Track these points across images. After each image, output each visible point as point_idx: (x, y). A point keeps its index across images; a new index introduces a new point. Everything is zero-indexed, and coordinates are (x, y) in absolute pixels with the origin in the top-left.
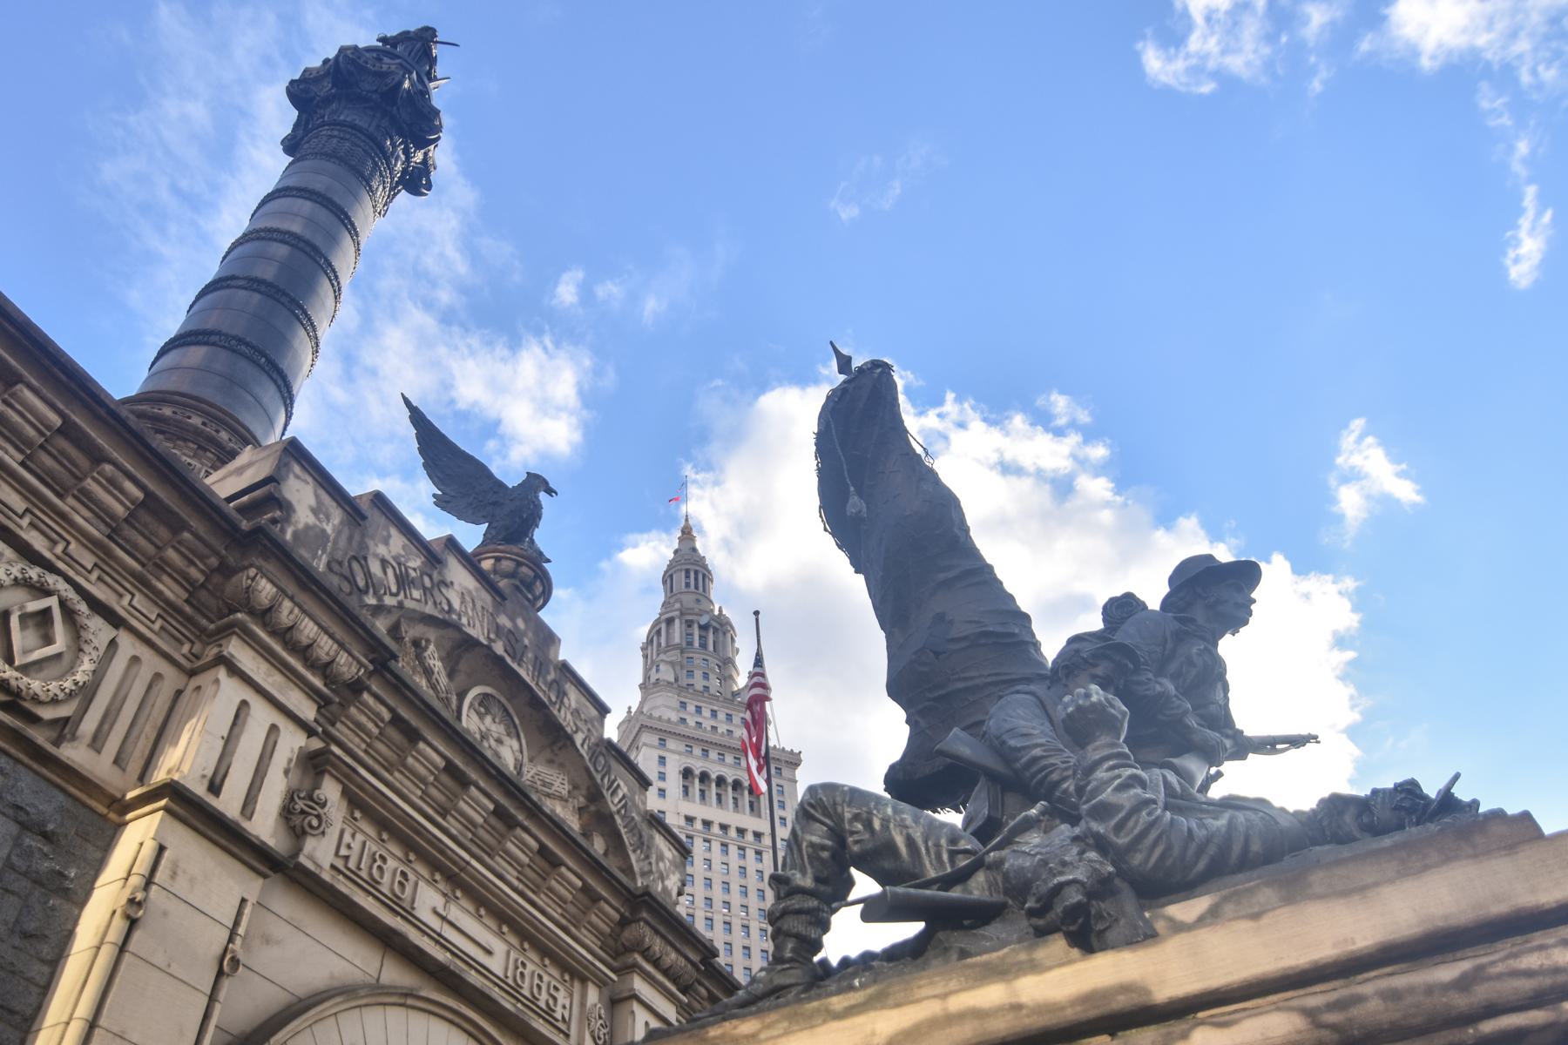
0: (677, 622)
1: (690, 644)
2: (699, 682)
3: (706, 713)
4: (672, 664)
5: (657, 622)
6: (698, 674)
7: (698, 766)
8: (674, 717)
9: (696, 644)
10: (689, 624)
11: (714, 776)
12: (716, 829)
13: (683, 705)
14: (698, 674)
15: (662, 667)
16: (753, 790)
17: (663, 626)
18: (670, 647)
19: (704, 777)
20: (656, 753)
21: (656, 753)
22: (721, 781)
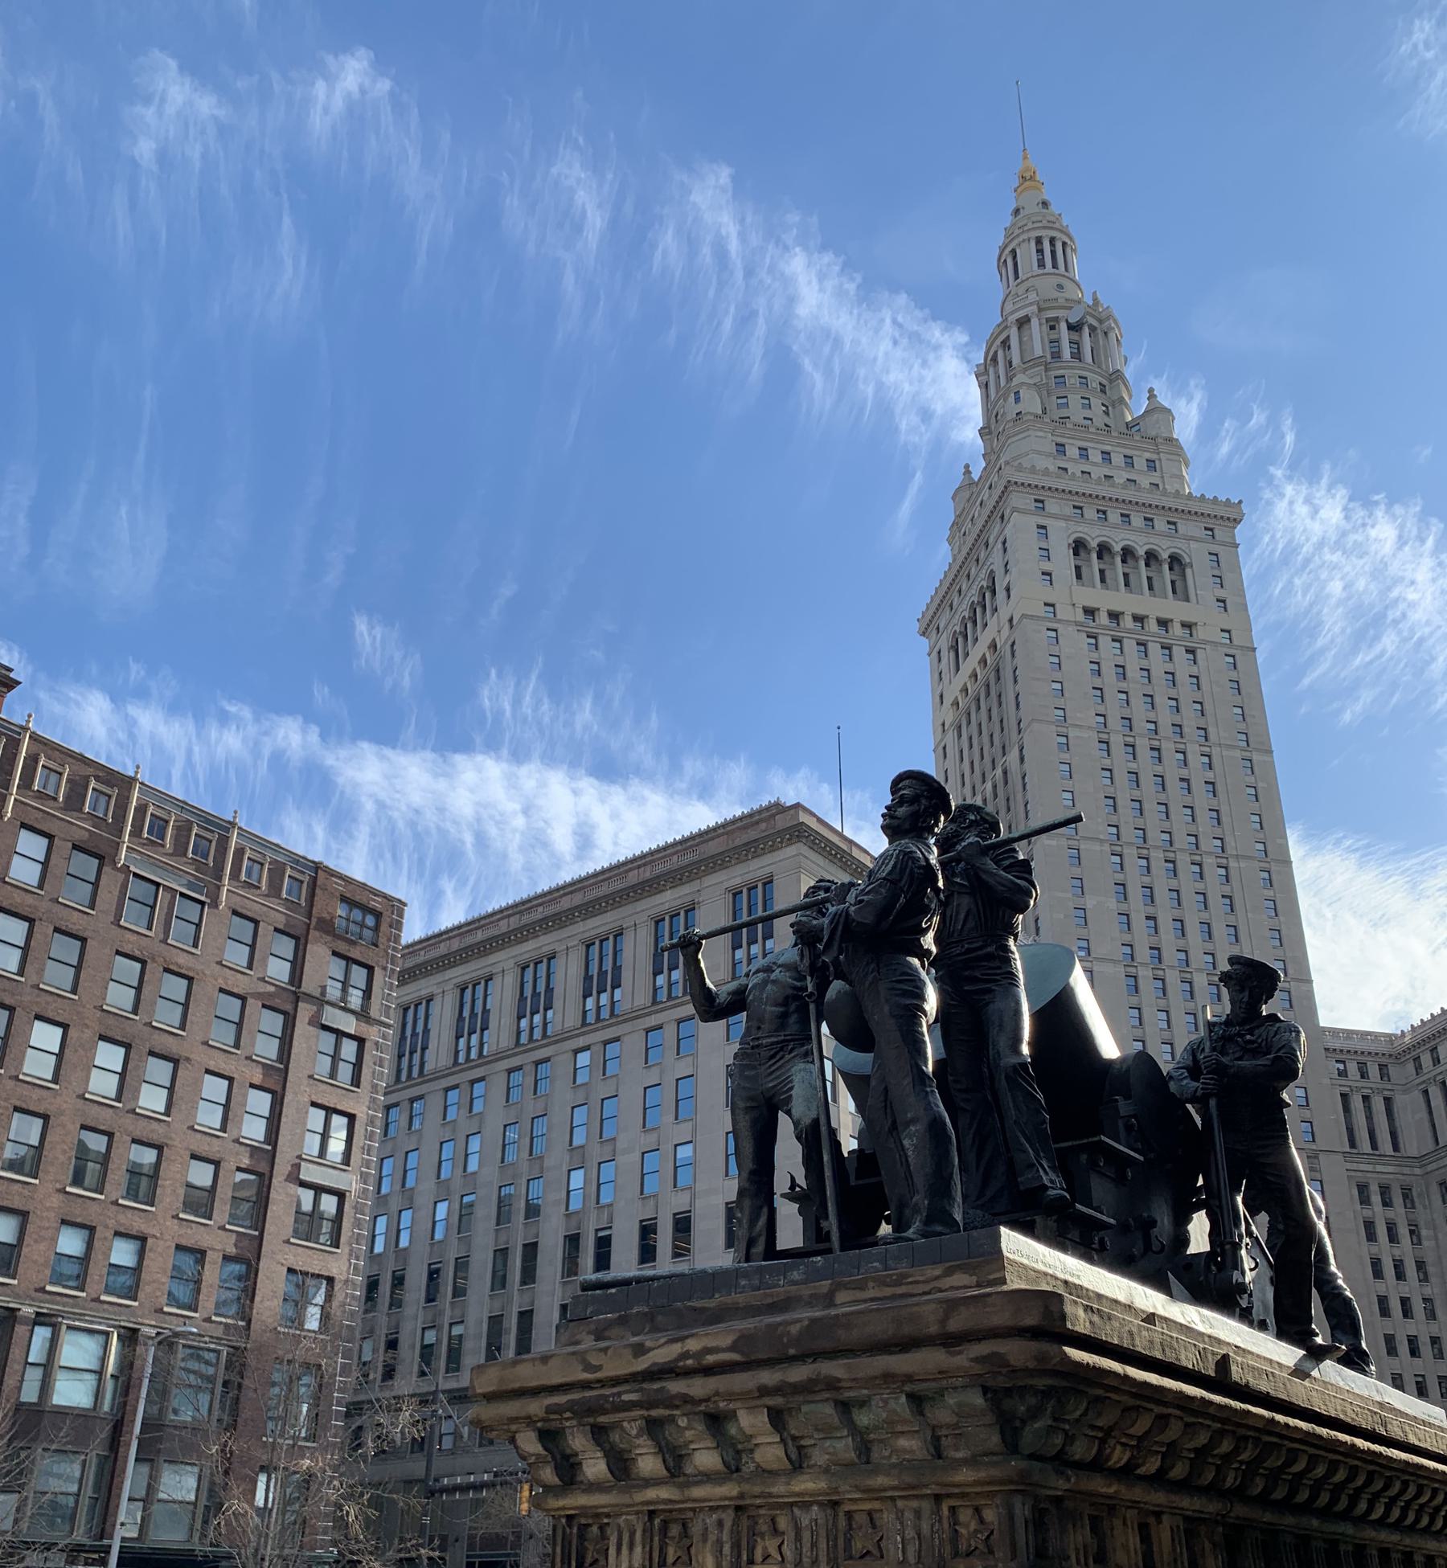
0: (1035, 322)
1: (1056, 355)
3: (1095, 456)
6: (1075, 400)
7: (1094, 536)
8: (1042, 463)
9: (1066, 353)
11: (1117, 548)
12: (1128, 622)
13: (1061, 447)
14: (1075, 400)
16: (1175, 561)
17: (1013, 332)
19: (1104, 550)
22: (1127, 554)
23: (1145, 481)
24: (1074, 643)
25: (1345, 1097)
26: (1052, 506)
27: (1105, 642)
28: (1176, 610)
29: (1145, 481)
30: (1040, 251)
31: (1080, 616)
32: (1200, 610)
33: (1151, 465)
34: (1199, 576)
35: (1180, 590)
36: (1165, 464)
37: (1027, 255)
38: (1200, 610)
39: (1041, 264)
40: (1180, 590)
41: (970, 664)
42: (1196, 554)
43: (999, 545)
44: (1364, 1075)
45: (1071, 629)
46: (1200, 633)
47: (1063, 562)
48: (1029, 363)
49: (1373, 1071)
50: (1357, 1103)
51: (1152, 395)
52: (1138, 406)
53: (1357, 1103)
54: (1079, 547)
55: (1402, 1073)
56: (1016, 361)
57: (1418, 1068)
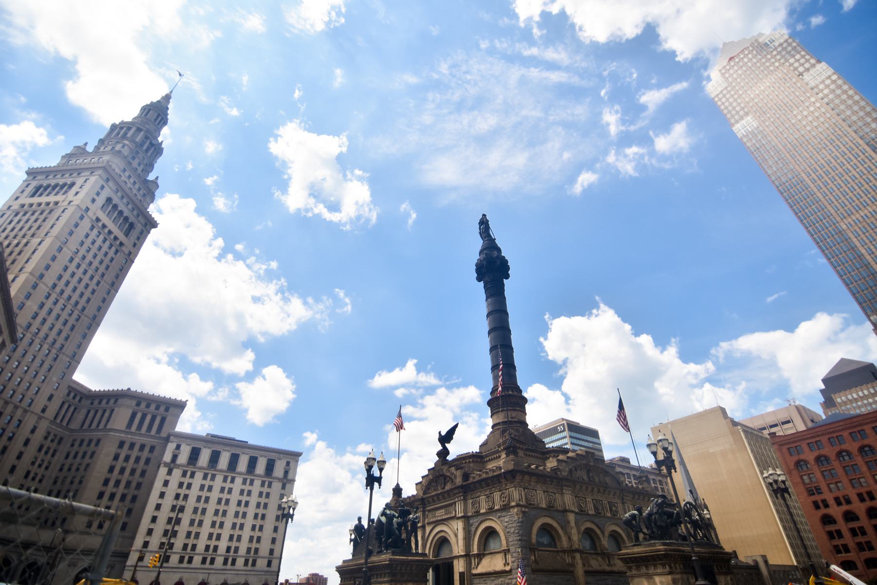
0: (142, 133)
1: (142, 145)
4: (131, 149)
7: (116, 200)
8: (117, 171)
9: (145, 147)
10: (147, 138)
13: (124, 170)
15: (126, 147)
16: (132, 226)
17: (134, 129)
25: (63, 403)
26: (111, 183)
27: (95, 231)
30: (157, 117)
31: (94, 218)
33: (144, 195)
34: (134, 234)
35: (127, 234)
36: (148, 199)
37: (152, 115)
39: (155, 120)
41: (36, 200)
42: (139, 227)
43: (84, 178)
44: (74, 398)
45: (88, 220)
46: (124, 248)
47: (101, 200)
48: (132, 140)
49: (78, 398)
50: (66, 406)
51: (157, 178)
53: (66, 406)
54: (109, 200)
55: (86, 403)
56: (129, 135)
57: (92, 403)
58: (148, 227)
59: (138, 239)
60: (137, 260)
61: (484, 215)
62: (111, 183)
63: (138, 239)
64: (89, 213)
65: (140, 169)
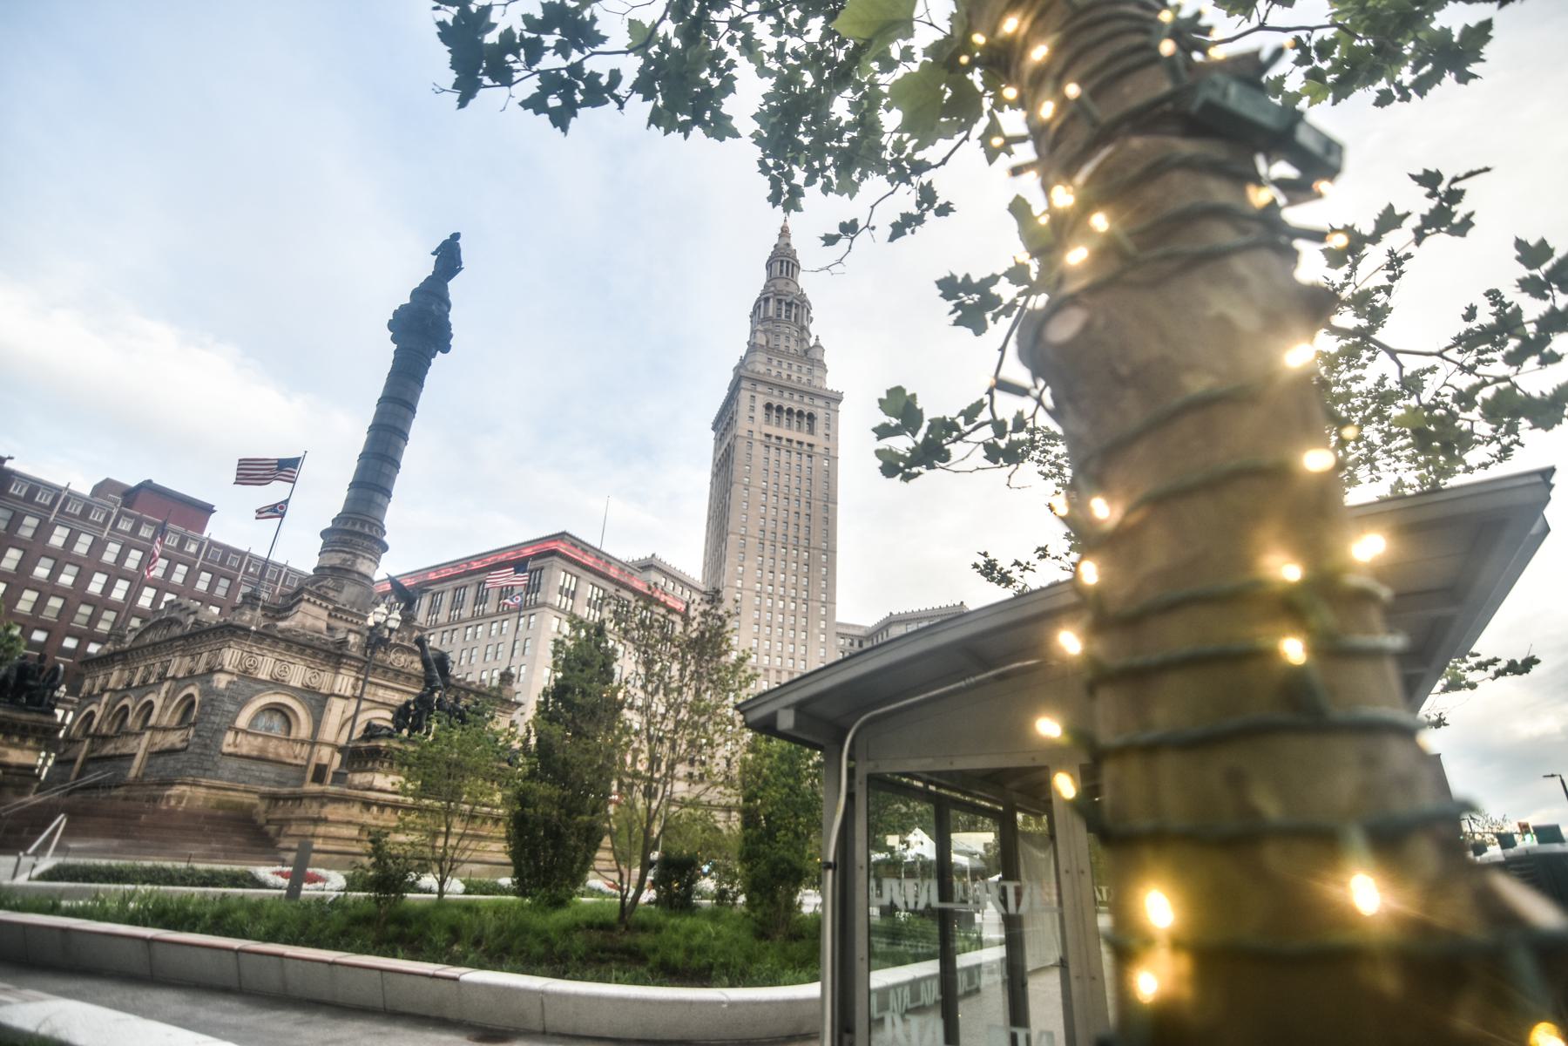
1: (779, 316)
2: (782, 343)
3: (785, 366)
5: (758, 300)
7: (776, 402)
10: (780, 301)
16: (811, 417)
18: (767, 319)
19: (779, 409)
20: (749, 394)
21: (749, 394)
22: (790, 411)
23: (804, 379)
24: (759, 450)
28: (806, 438)
29: (804, 379)
32: (818, 440)
35: (811, 431)
38: (818, 440)
40: (811, 431)
42: (820, 414)
46: (816, 449)
52: (812, 342)
54: (768, 407)
58: (832, 405)
59: (828, 426)
60: (840, 454)
61: (456, 236)
62: (760, 388)
63: (828, 426)
64: (756, 436)
65: (792, 344)
